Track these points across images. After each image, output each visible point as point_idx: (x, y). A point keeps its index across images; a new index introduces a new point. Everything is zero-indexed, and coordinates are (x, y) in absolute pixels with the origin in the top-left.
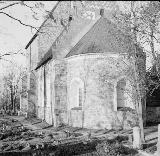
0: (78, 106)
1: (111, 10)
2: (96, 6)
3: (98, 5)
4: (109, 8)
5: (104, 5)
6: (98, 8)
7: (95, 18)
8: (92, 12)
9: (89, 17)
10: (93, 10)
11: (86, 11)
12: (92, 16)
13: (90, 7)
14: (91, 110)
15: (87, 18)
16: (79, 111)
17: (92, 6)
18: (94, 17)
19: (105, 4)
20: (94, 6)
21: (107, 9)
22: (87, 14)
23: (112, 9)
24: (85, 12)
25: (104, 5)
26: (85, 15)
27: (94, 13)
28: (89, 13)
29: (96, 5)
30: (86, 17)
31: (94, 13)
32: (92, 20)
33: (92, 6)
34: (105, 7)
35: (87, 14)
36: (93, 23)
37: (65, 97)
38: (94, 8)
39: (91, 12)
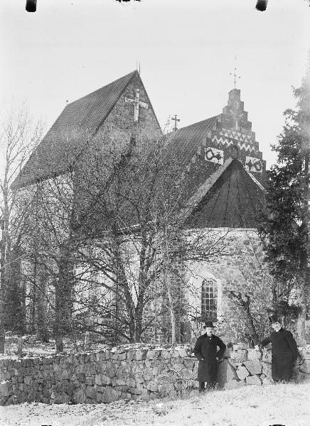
1: (246, 149)
7: (224, 162)
8: (219, 151)
9: (215, 160)
12: (218, 157)
13: (218, 141)
15: (211, 161)
17: (221, 139)
18: (221, 161)
19: (239, 138)
23: (249, 146)
27: (222, 153)
28: (216, 151)
30: (211, 158)
34: (239, 144)
38: (224, 143)
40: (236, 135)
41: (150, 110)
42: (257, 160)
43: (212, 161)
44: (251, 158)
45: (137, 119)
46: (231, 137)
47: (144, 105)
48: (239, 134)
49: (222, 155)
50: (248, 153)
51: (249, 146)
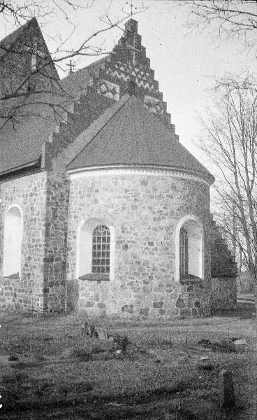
1: (146, 87)
2: (123, 75)
3: (126, 74)
4: (142, 83)
5: (135, 75)
7: (121, 96)
9: (110, 95)
10: (119, 81)
11: (105, 81)
12: (114, 92)
14: (130, 281)
15: (106, 95)
16: (103, 282)
17: (116, 73)
18: (117, 97)
20: (119, 74)
21: (139, 85)
22: (107, 88)
23: (147, 85)
24: (104, 83)
25: (135, 75)
26: (103, 88)
28: (112, 85)
29: (121, 71)
30: (105, 93)
32: (115, 101)
33: (116, 73)
35: (107, 88)
36: (117, 106)
37: (62, 254)
38: (119, 77)
39: (113, 85)
40: (133, 70)
42: (157, 100)
43: (106, 95)
44: (150, 98)
46: (128, 71)
48: (137, 70)
49: (118, 90)
50: (146, 92)
51: (147, 85)
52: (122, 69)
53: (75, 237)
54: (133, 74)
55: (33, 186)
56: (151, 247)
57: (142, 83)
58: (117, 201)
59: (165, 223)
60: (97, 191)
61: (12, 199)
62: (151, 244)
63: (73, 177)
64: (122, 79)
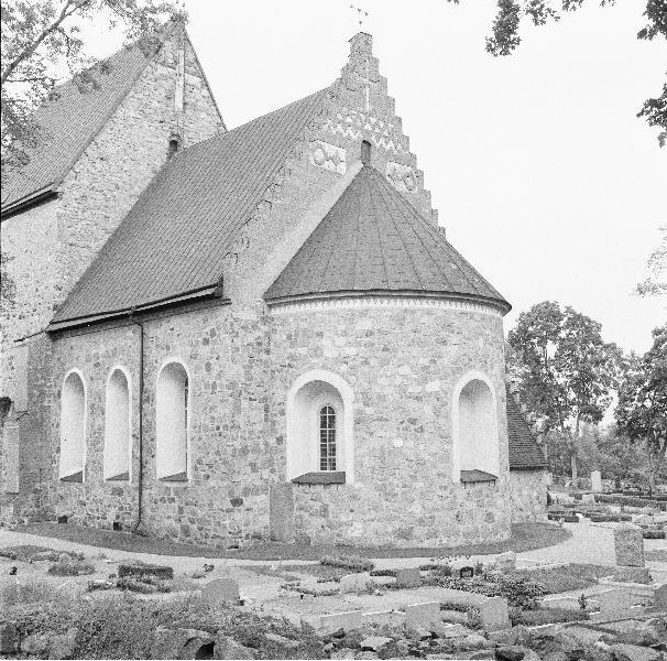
0: (315, 467)
1: (388, 147)
2: (349, 130)
3: (356, 129)
6: (354, 137)
9: (329, 165)
10: (343, 143)
17: (339, 126)
18: (343, 166)
21: (378, 145)
23: (391, 144)
26: (319, 154)
28: (331, 149)
31: (342, 154)
34: (373, 138)
38: (345, 135)
41: (205, 92)
45: (180, 105)
47: (195, 80)
50: (388, 155)
51: (391, 144)
52: (349, 120)
53: (283, 413)
54: (368, 127)
55: (208, 329)
56: (413, 427)
57: (382, 141)
58: (351, 351)
59: (434, 386)
60: (320, 334)
61: (168, 348)
62: (413, 422)
63: (276, 312)
64: (349, 138)
